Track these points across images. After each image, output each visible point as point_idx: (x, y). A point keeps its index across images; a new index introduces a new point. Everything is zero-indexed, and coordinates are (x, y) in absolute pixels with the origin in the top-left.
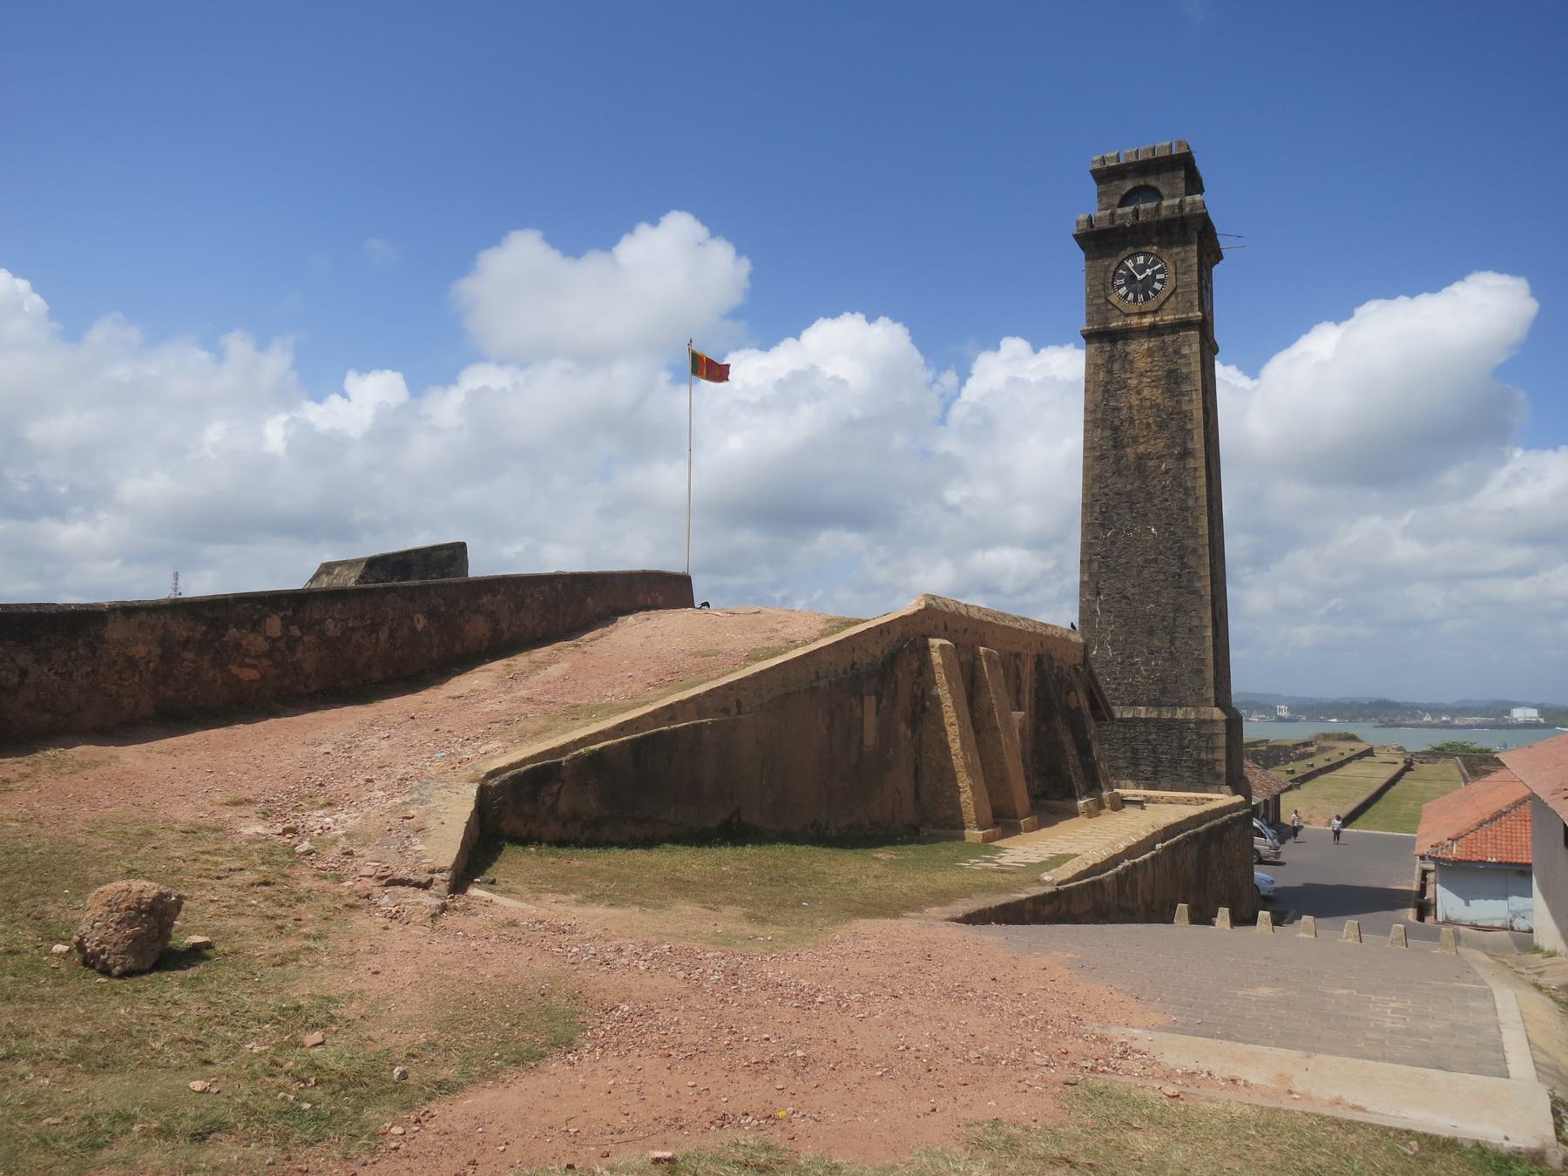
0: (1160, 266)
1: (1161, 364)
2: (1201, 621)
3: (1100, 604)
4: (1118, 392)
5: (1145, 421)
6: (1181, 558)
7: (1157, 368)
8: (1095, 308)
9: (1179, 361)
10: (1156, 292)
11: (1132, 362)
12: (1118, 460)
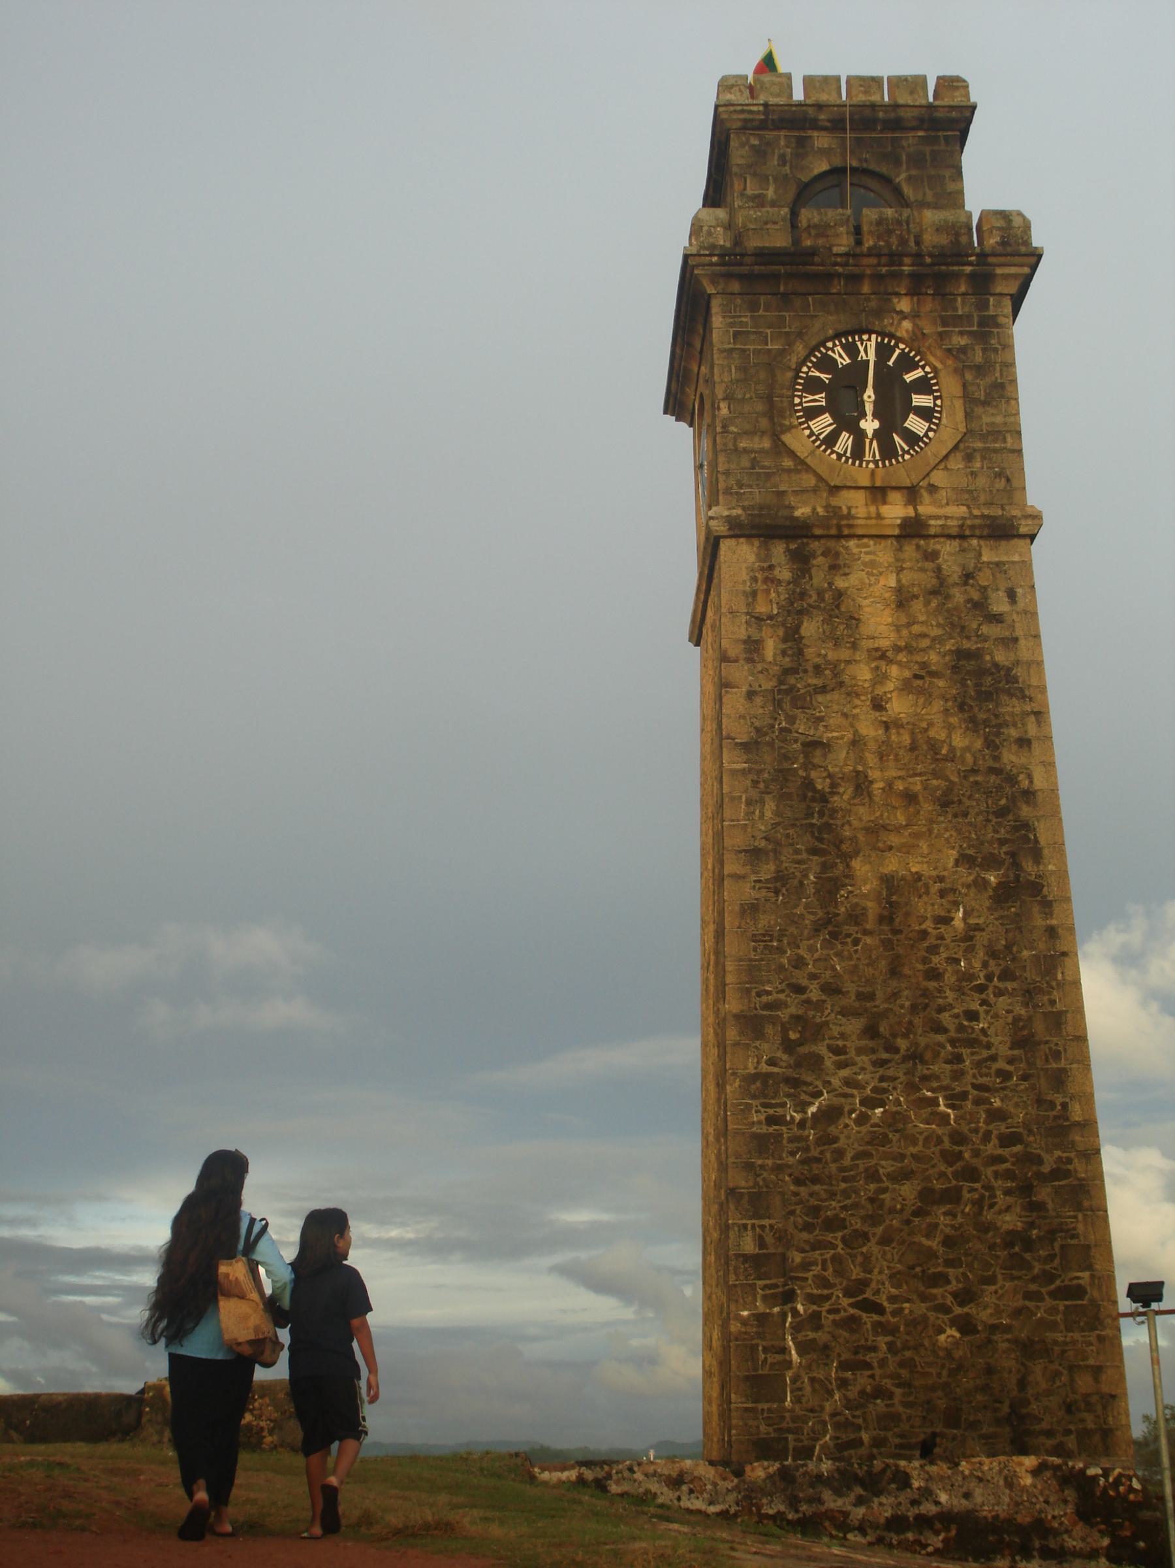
0: (918, 373)
1: (939, 632)
2: (1097, 1380)
3: (796, 1328)
4: (820, 698)
5: (900, 786)
6: (1026, 1189)
7: (925, 643)
8: (745, 462)
9: (985, 629)
10: (912, 438)
11: (853, 620)
12: (830, 888)
